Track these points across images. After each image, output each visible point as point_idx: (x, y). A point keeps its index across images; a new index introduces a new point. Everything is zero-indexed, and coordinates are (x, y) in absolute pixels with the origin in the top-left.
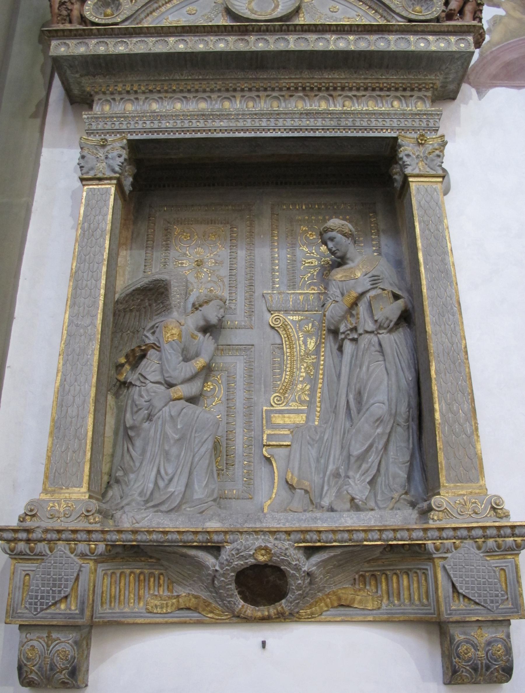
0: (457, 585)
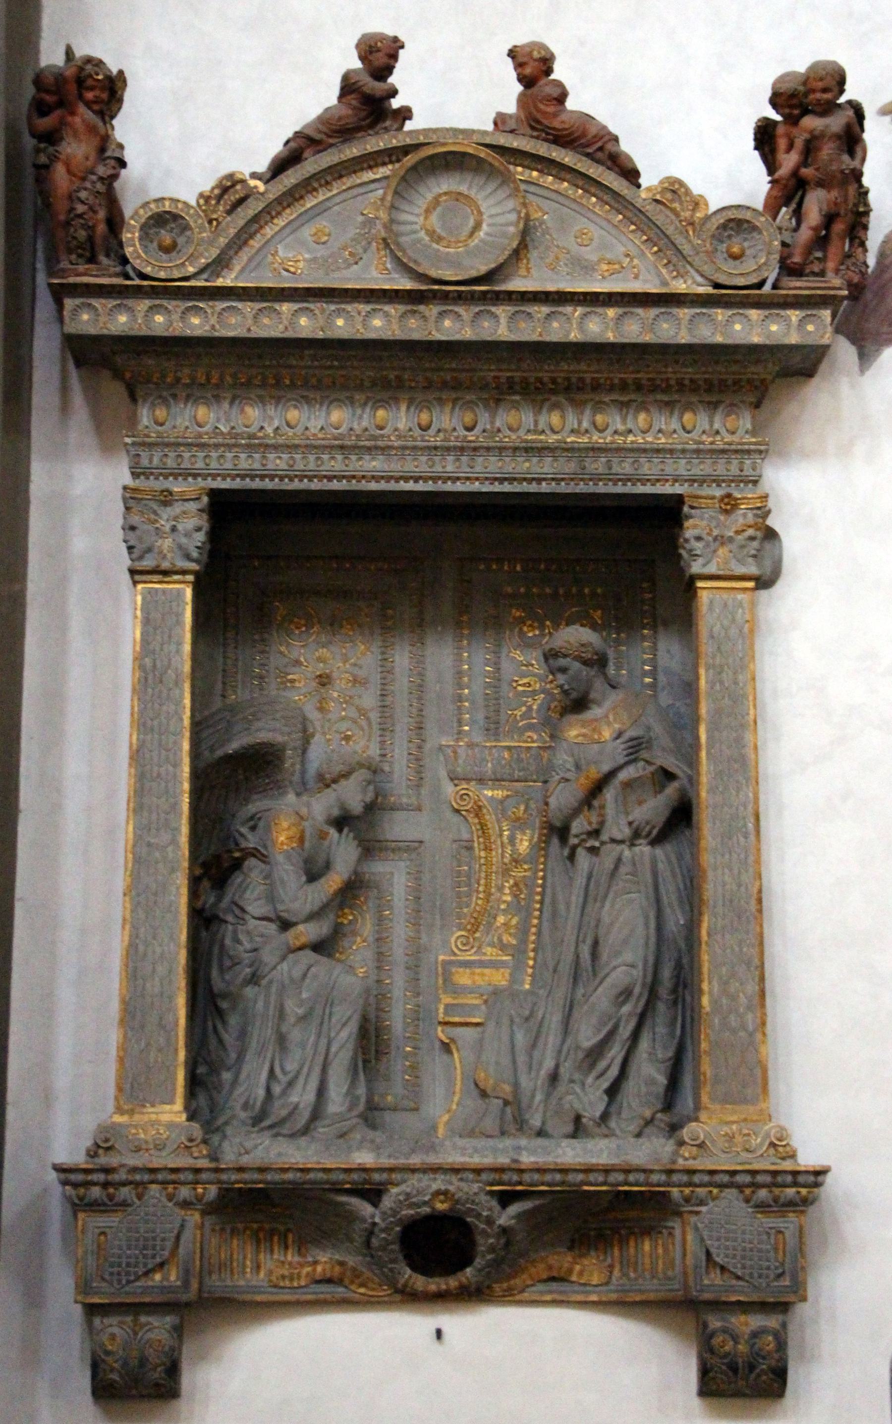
0: (713, 1251)
